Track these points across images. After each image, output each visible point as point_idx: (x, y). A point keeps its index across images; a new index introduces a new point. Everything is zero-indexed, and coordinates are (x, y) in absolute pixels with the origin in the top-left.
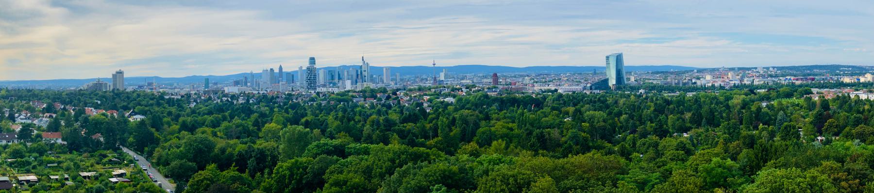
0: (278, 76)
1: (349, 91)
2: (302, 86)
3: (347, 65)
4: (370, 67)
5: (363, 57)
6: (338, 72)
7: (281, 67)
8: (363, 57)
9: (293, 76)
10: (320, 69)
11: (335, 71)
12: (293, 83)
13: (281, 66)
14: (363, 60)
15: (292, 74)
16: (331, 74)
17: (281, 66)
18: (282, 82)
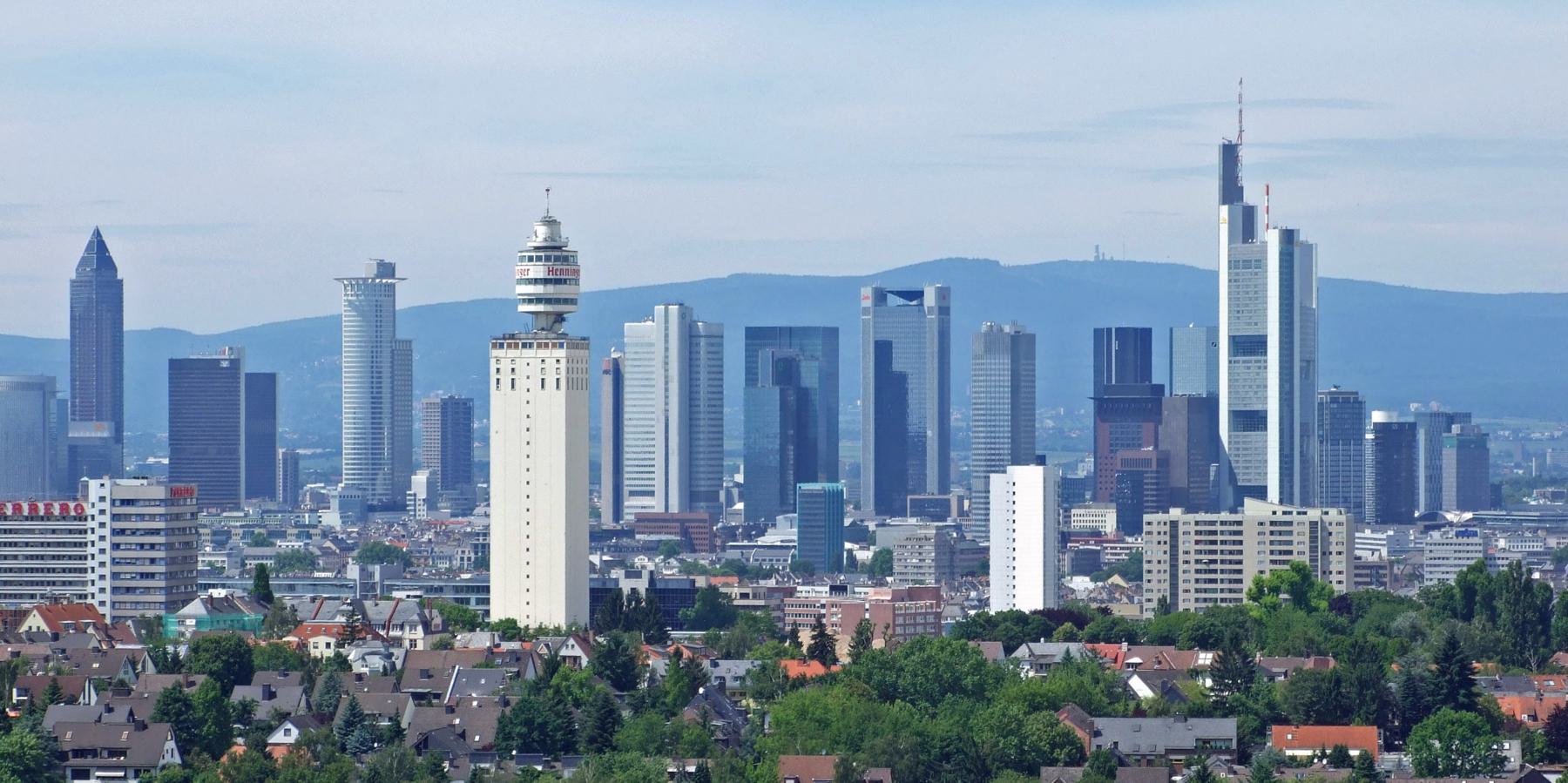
0: (64, 390)
1: (1019, 628)
2: (381, 530)
3: (1009, 258)
4: (1320, 280)
5: (1230, 154)
6: (883, 350)
7: (99, 255)
8: (1230, 154)
9: (264, 386)
10: (638, 303)
11: (831, 334)
12: (261, 487)
13: (97, 233)
14: (1231, 191)
15: (250, 366)
16: (786, 373)
17: (97, 233)
18: (117, 472)
